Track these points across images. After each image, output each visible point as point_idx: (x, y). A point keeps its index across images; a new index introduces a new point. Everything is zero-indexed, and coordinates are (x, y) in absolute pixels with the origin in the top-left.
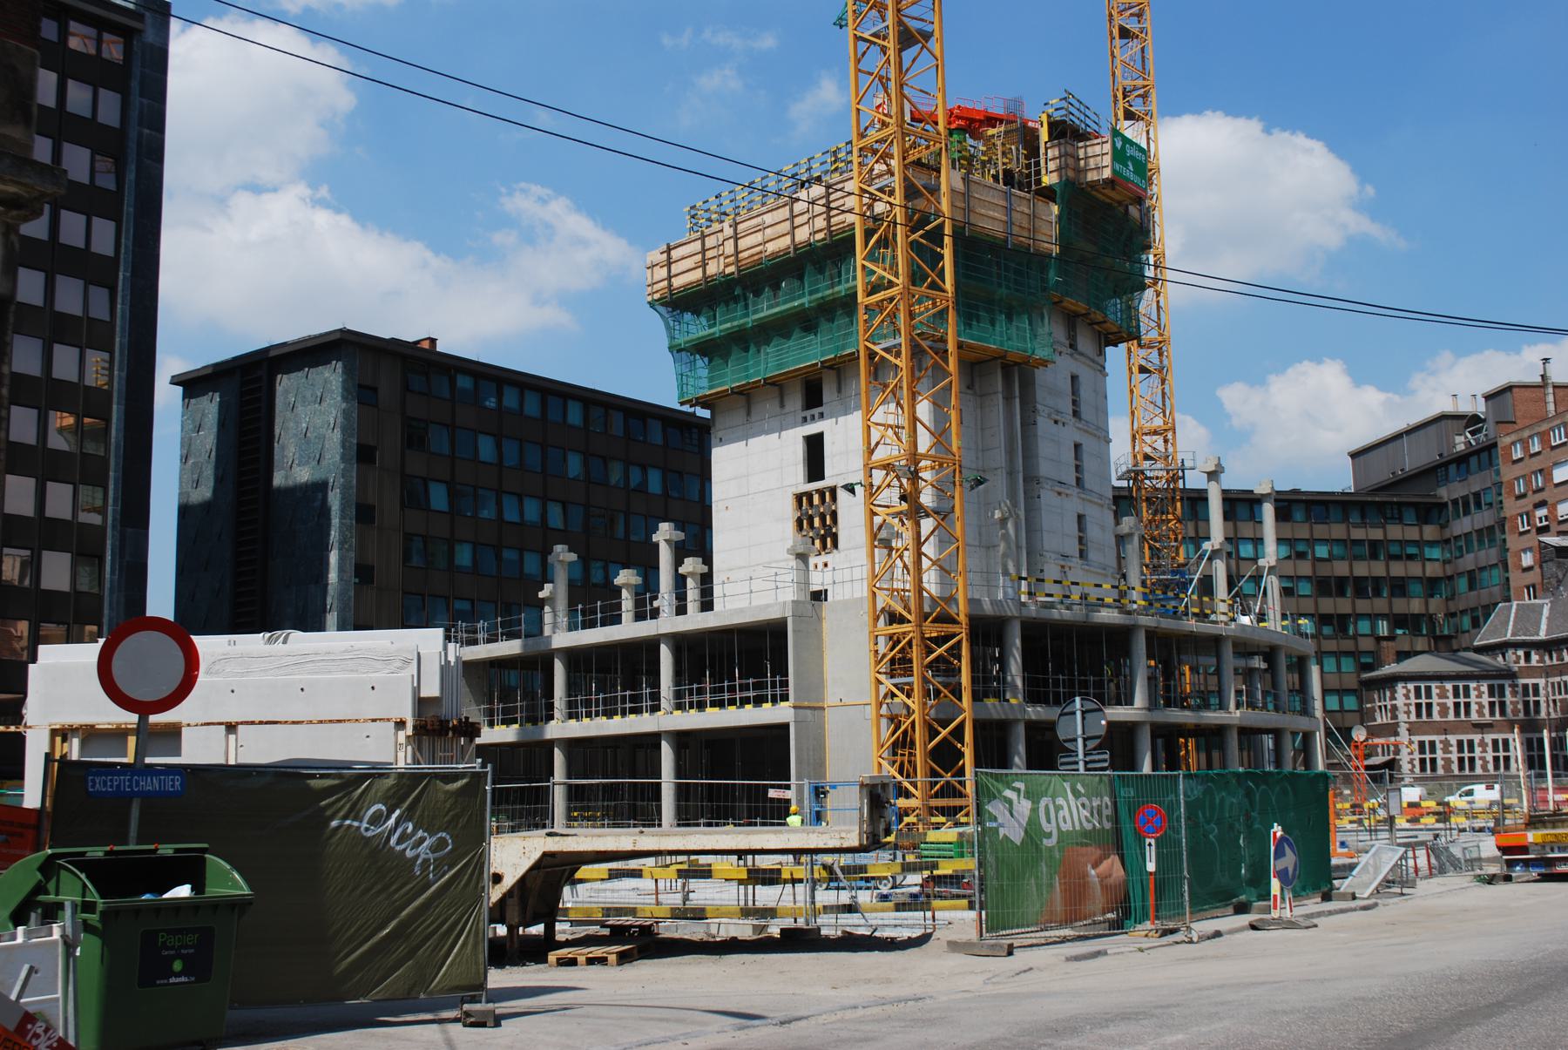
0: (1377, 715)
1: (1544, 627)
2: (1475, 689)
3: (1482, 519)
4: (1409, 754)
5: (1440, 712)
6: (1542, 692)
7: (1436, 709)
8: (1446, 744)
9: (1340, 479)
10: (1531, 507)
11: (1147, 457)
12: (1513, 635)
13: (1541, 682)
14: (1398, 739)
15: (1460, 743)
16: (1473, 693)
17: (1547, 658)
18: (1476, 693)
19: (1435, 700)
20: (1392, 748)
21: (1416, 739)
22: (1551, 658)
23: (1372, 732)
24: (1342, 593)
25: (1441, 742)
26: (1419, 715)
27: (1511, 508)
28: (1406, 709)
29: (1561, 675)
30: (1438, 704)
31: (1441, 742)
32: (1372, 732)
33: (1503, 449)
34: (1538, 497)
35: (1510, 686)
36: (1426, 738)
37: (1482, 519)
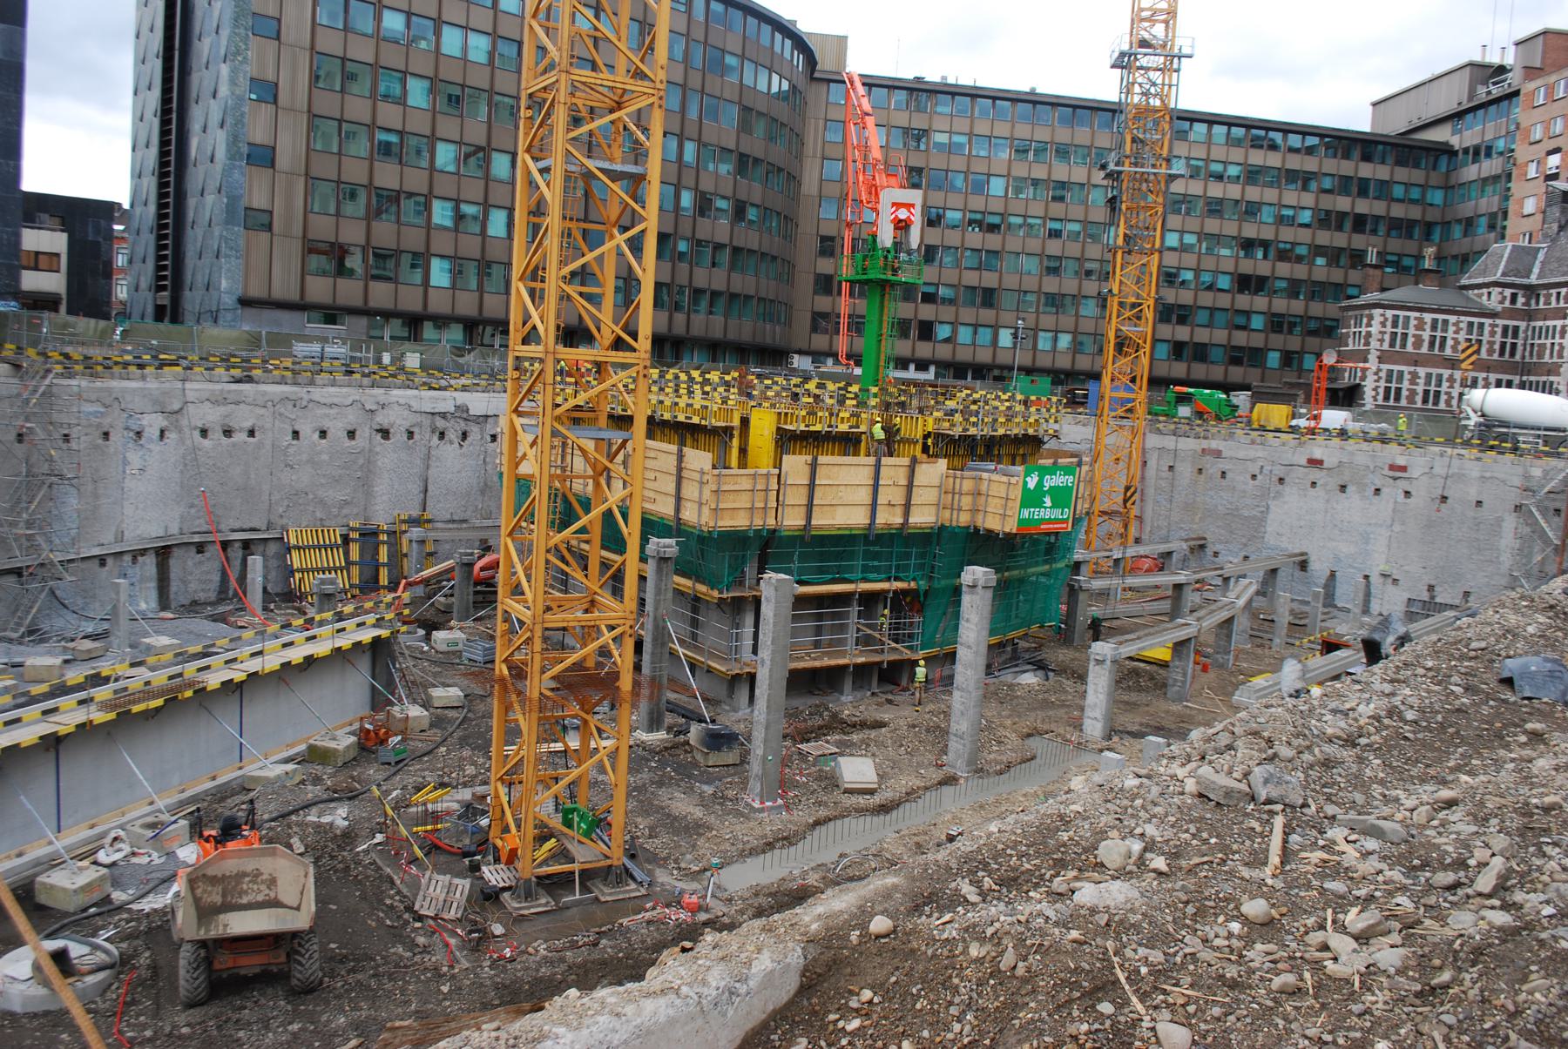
0: (1350, 341)
1: (1536, 270)
2: (1454, 324)
3: (1489, 167)
4: (1376, 381)
5: (1414, 344)
6: (1521, 335)
7: (1410, 340)
8: (1414, 376)
9: (1362, 122)
10: (1543, 154)
11: (1144, 44)
12: (1504, 274)
13: (1522, 325)
14: (1367, 365)
15: (1429, 376)
16: (1451, 329)
17: (1533, 302)
18: (1454, 328)
19: (1412, 331)
20: (1359, 374)
21: (1385, 367)
22: (1537, 303)
23: (1342, 357)
24: (1340, 228)
25: (1410, 373)
26: (1392, 344)
27: (1522, 152)
28: (1380, 337)
29: (1545, 319)
30: (1414, 336)
31: (1410, 373)
32: (1342, 357)
33: (1525, 94)
34: (1553, 144)
35: (1490, 325)
36: (1396, 368)
37: (1489, 167)
